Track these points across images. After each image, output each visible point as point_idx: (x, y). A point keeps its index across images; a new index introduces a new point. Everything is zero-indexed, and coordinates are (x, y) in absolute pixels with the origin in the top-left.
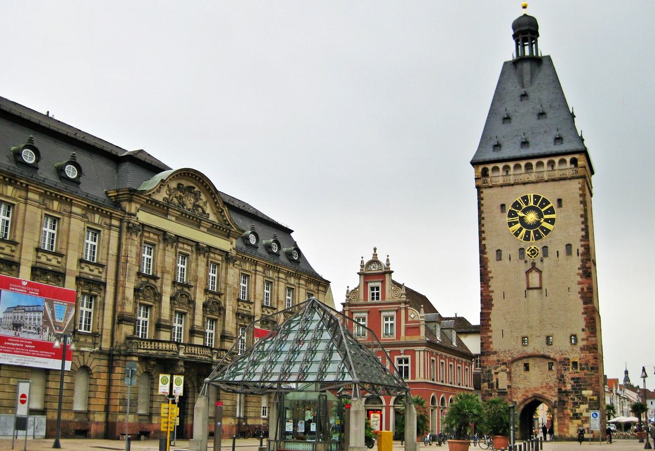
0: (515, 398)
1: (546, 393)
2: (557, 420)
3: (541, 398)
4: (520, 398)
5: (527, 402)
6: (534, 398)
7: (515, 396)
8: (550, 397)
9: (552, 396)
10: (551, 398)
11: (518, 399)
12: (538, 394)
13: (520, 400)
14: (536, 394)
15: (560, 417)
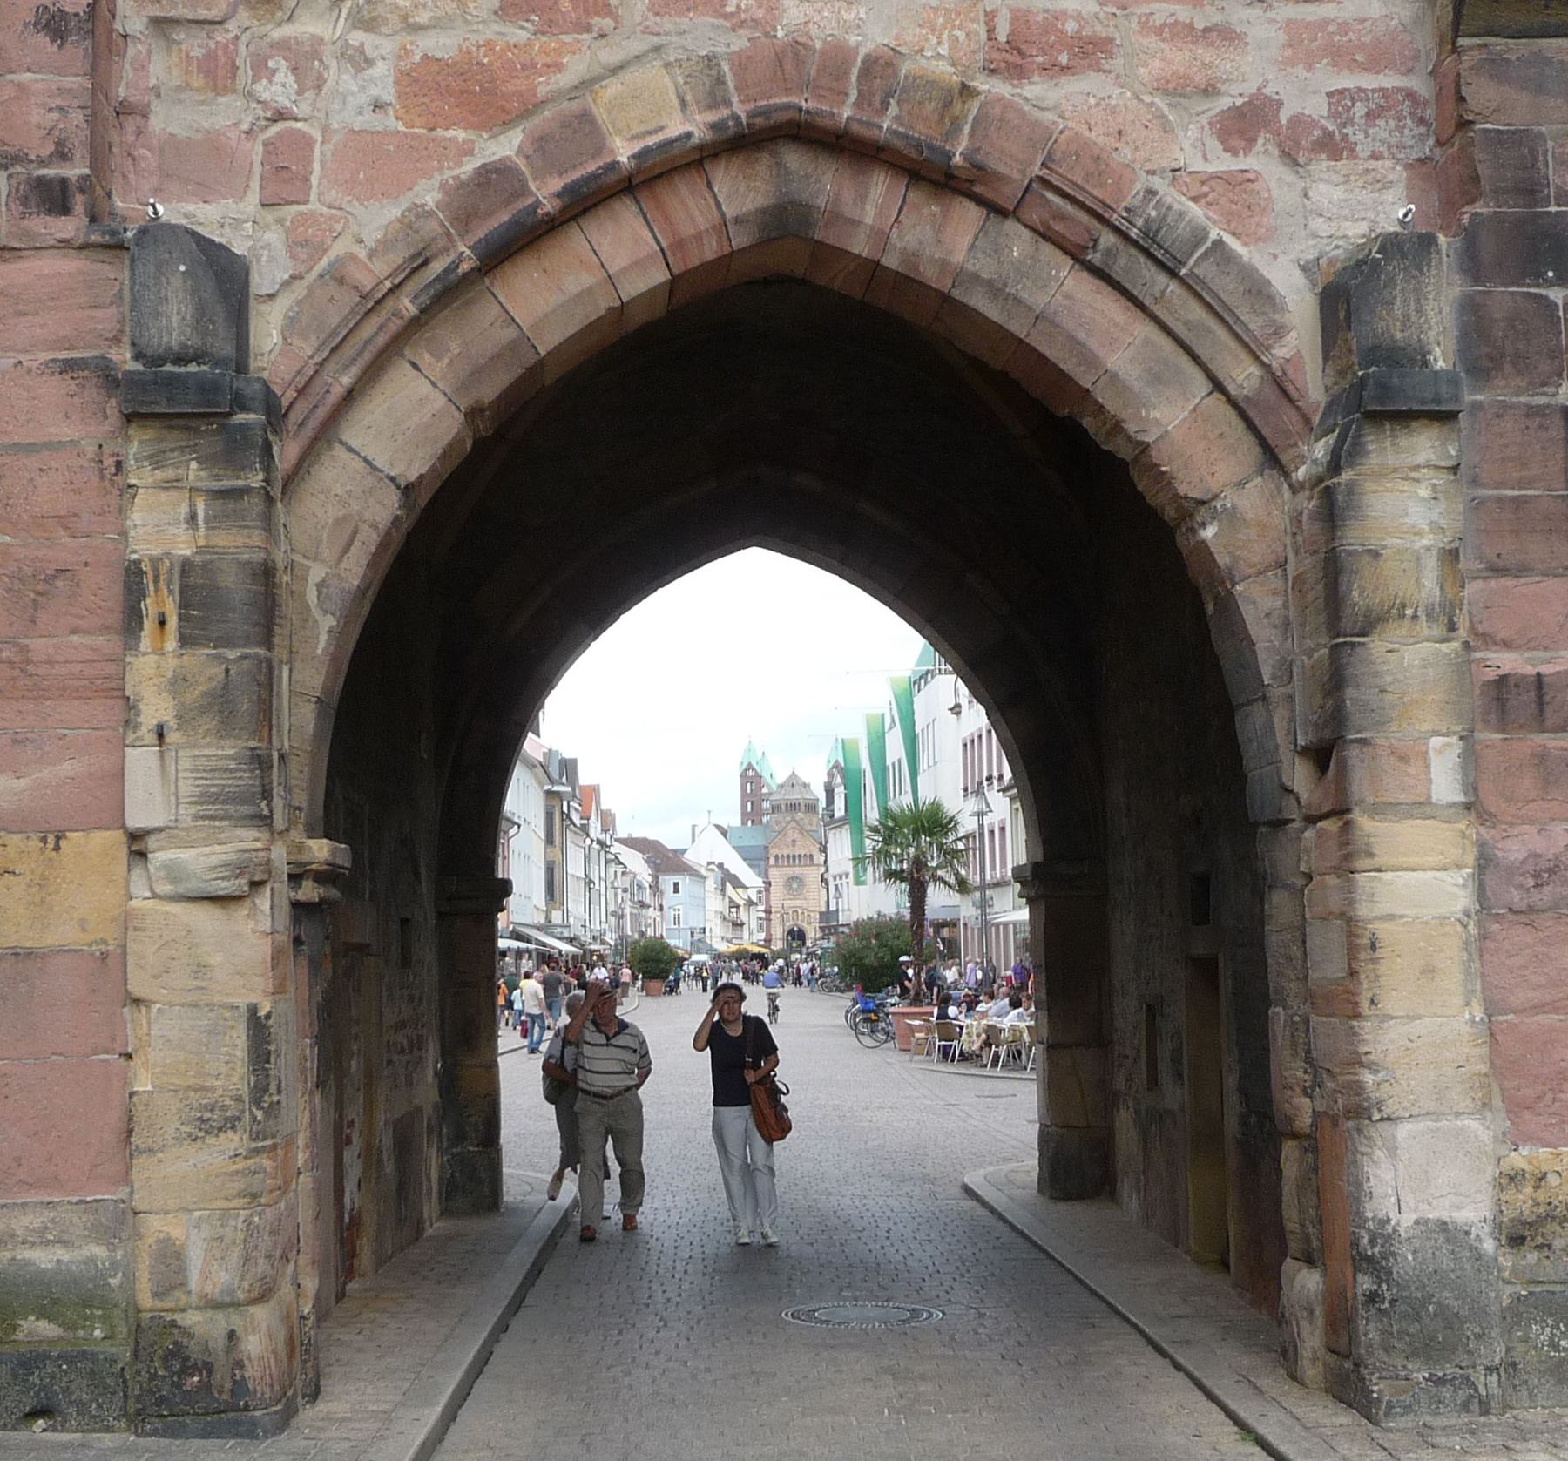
0: (205, 164)
1: (1090, 51)
2: (1444, 780)
3: (932, 175)
4: (370, 161)
5: (550, 302)
6: (739, 193)
7: (227, 115)
8: (1194, 147)
9: (1244, 124)
10: (1236, 190)
11: (284, 178)
12: (879, 67)
13: (369, 228)
14: (836, 60)
15: (1512, 704)
